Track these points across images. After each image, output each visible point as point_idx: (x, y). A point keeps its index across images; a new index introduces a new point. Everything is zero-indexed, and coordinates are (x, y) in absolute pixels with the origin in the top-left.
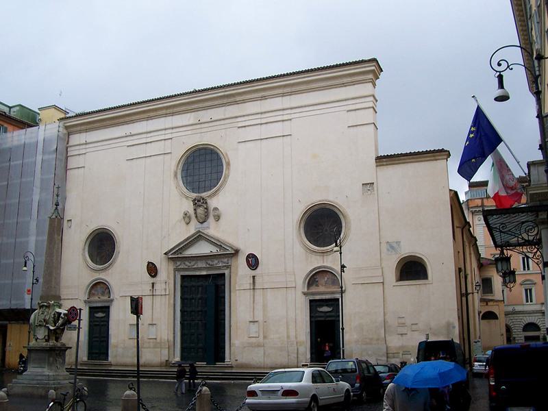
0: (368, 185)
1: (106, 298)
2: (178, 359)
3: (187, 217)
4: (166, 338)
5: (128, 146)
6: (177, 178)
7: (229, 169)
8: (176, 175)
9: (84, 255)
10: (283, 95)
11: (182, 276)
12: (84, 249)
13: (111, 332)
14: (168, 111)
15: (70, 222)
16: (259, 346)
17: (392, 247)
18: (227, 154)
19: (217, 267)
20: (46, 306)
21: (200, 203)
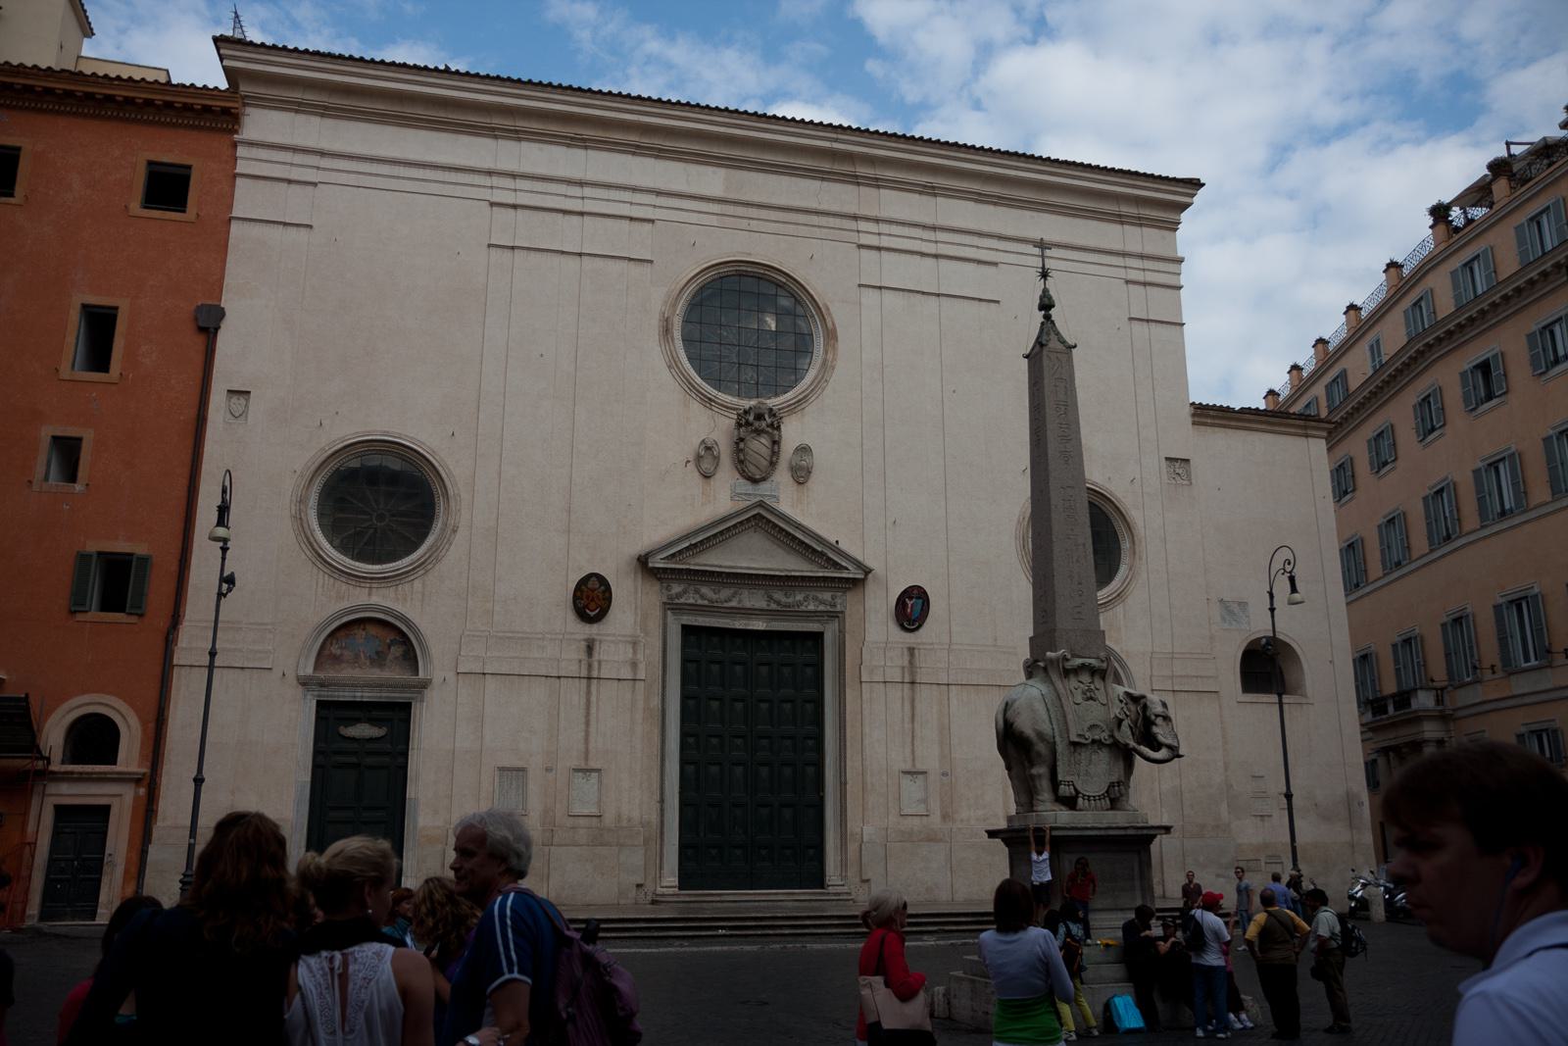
0: (1178, 463)
1: (393, 673)
2: (671, 879)
3: (705, 460)
4: (636, 814)
5: (492, 204)
6: (673, 340)
7: (834, 348)
8: (666, 330)
9: (299, 520)
10: (980, 198)
11: (684, 627)
12: (302, 501)
13: (410, 792)
14: (646, 141)
15: (238, 403)
16: (932, 838)
17: (1232, 609)
18: (828, 309)
19: (803, 612)
20: (1093, 672)
21: (764, 424)
